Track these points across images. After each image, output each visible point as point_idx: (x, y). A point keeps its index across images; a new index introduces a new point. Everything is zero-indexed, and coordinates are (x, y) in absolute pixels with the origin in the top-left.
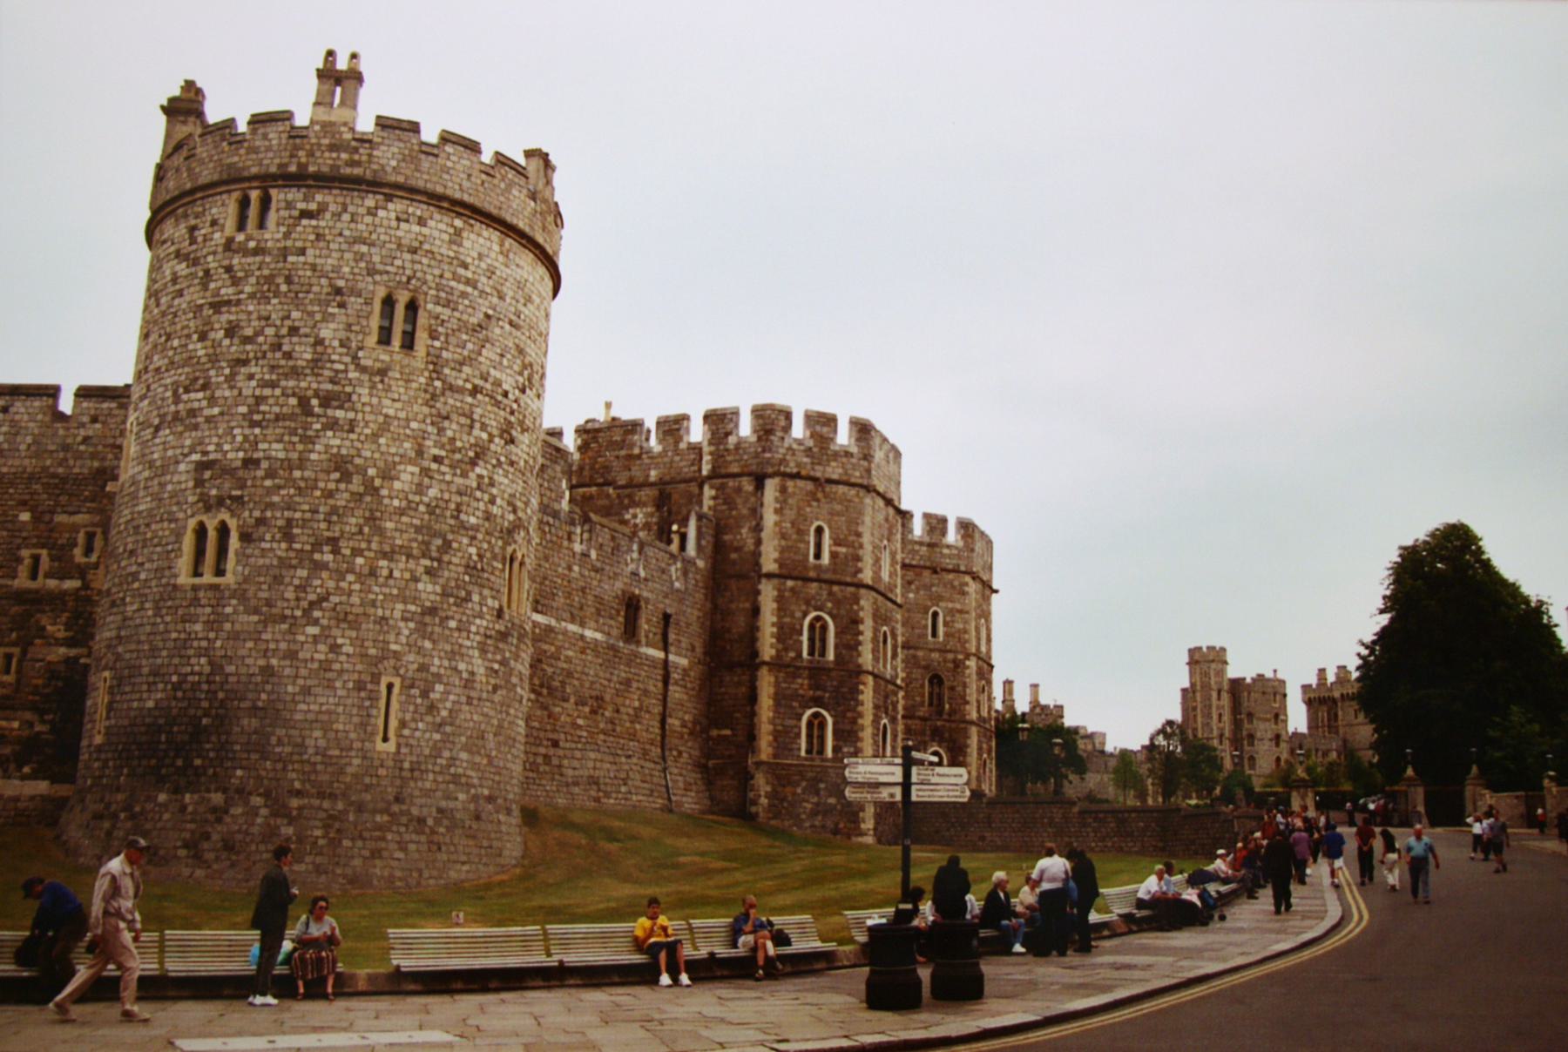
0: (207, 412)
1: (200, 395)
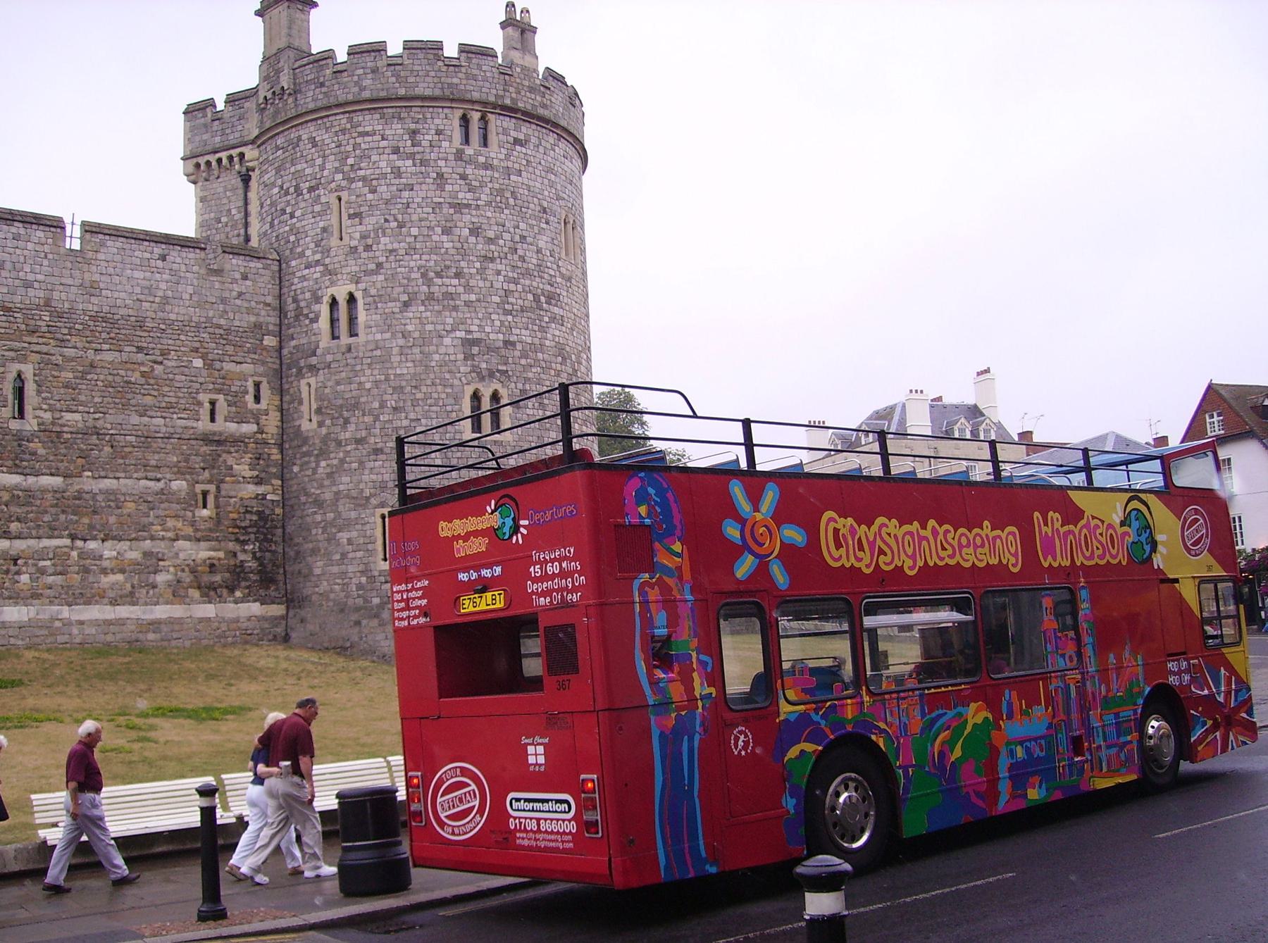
0: (465, 297)
1: (455, 282)
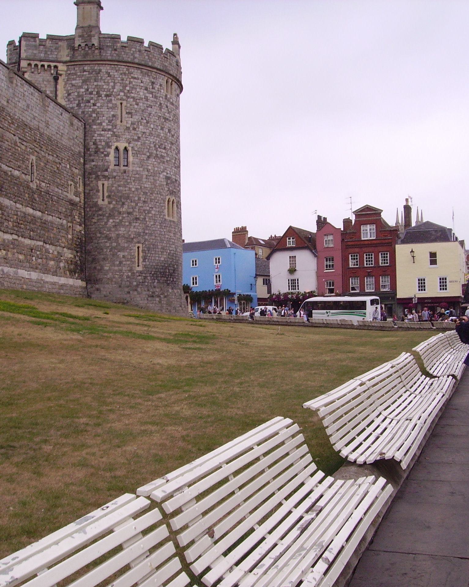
1: (164, 151)
